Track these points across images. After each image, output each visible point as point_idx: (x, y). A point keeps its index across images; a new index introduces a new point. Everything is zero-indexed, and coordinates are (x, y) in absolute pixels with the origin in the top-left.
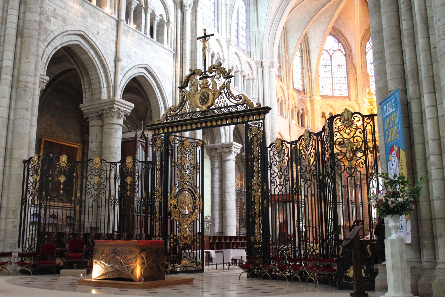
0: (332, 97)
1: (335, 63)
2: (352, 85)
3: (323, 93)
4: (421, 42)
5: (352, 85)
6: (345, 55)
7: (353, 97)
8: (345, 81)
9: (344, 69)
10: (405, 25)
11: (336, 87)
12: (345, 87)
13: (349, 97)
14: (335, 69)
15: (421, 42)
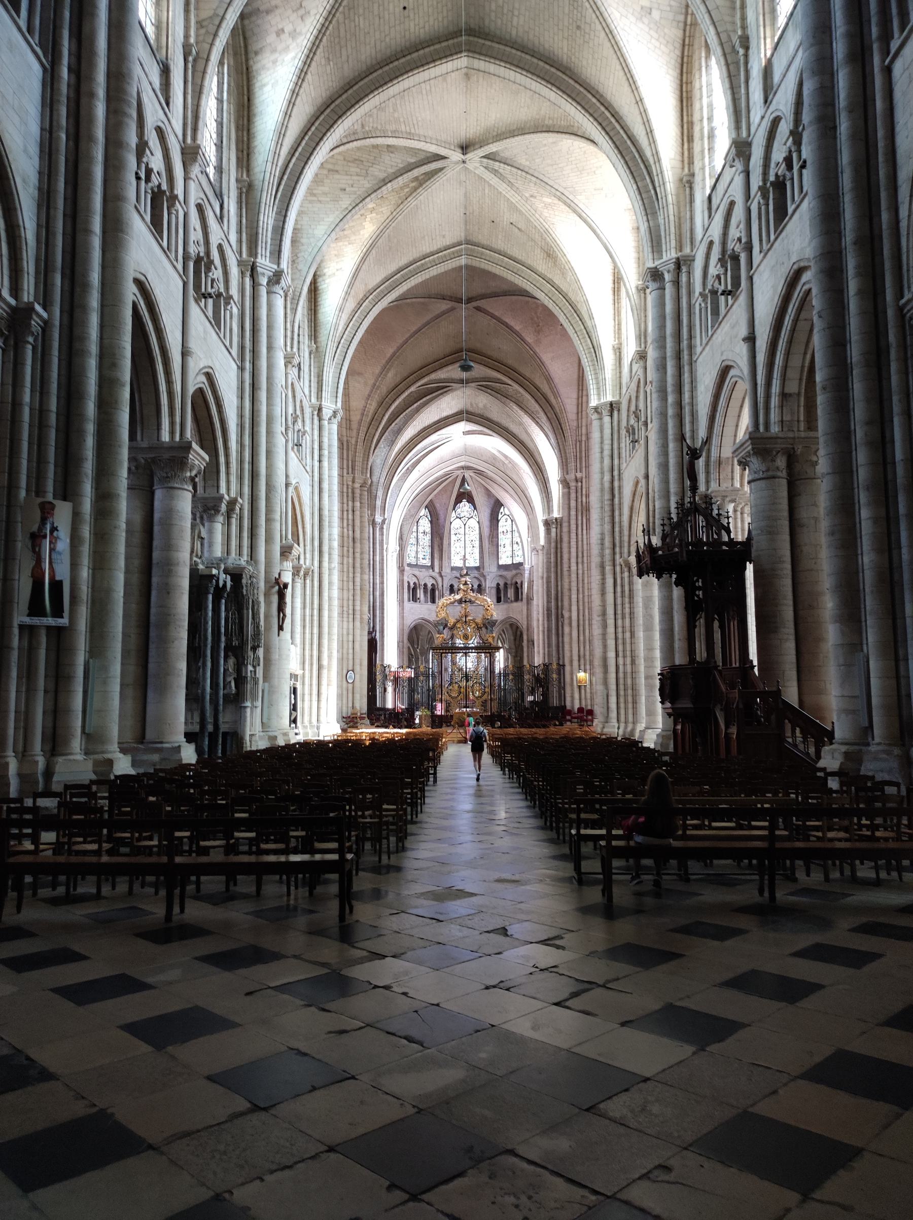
0: (416, 566)
1: (421, 529)
2: (436, 555)
3: (408, 561)
4: (587, 647)
5: (436, 555)
6: (431, 522)
7: (437, 569)
8: (428, 550)
9: (428, 537)
10: (581, 638)
11: (421, 556)
12: (428, 557)
13: (432, 567)
14: (421, 536)
15: (587, 647)
